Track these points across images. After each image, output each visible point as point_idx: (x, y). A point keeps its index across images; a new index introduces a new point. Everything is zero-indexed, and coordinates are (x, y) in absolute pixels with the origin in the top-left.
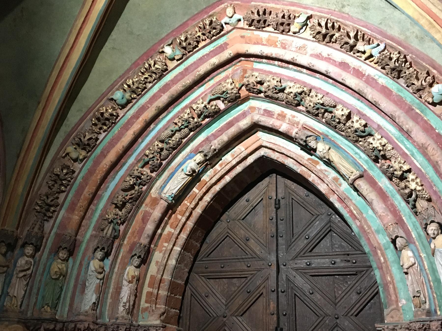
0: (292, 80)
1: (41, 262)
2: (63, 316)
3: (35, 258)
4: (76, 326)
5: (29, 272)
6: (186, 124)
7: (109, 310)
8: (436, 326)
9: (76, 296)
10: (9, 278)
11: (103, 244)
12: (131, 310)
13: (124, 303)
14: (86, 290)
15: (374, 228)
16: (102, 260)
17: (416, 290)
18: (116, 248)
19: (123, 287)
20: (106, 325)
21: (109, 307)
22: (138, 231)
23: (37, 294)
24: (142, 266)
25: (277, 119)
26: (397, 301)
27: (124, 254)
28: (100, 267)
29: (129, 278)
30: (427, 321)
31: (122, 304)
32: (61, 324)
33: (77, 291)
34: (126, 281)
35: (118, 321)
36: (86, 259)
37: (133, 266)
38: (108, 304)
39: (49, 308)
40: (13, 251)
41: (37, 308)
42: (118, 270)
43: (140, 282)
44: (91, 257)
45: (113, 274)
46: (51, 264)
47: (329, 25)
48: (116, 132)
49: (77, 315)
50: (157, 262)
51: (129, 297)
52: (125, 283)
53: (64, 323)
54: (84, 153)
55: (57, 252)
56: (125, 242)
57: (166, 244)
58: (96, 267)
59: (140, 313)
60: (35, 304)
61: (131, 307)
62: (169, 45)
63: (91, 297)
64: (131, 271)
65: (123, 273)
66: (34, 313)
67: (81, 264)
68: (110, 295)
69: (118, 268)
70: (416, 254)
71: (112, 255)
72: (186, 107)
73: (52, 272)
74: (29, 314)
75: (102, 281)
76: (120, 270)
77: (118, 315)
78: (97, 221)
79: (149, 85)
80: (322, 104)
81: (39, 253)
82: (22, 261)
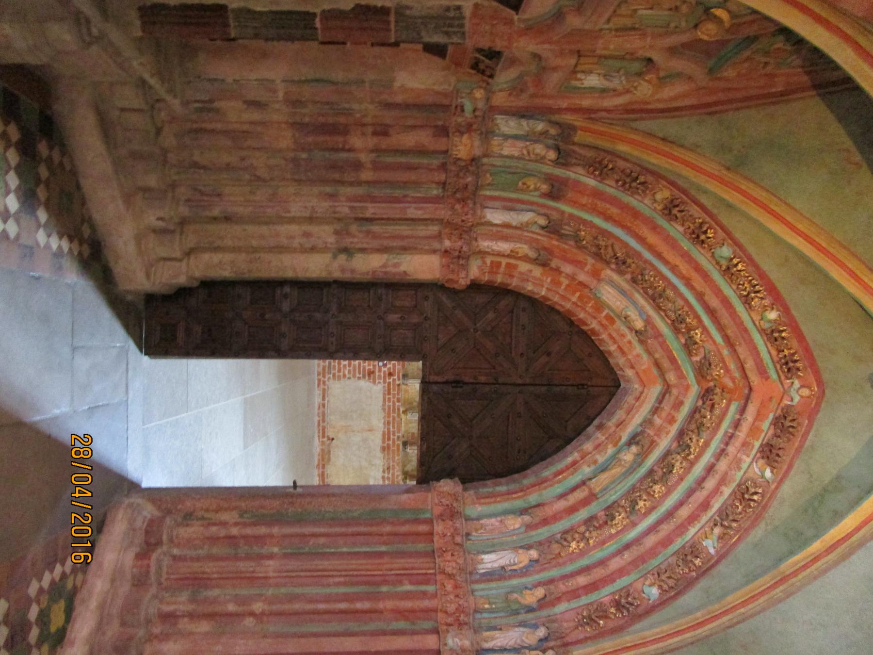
0: (707, 444)
6: (680, 319)
15: (544, 492)
25: (670, 414)
26: (480, 504)
47: (752, 504)
48: (682, 244)
50: (531, 271)
54: (659, 208)
57: (549, 280)
62: (779, 316)
70: (516, 532)
72: (700, 321)
79: (734, 287)
80: (671, 471)
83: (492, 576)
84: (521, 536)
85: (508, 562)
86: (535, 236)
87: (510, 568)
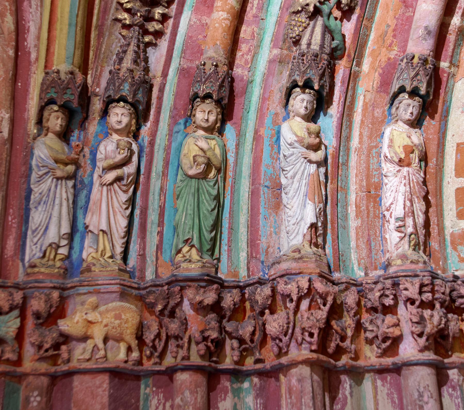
1: (156, 147)
2: (236, 274)
3: (140, 140)
4: (274, 290)
5: (130, 169)
7: (357, 246)
9: (261, 217)
10: (85, 192)
11: (304, 72)
12: (422, 238)
13: (397, 219)
14: (283, 195)
16: (312, 117)
18: (343, 82)
19: (386, 181)
20: (361, 285)
21: (357, 239)
22: (394, 30)
23: (161, 223)
24: (425, 123)
27: (369, 96)
28: (309, 133)
29: (396, 153)
31: (393, 224)
32: (235, 291)
33: (262, 203)
34: (392, 162)
35: (391, 270)
36: (268, 121)
37: (400, 123)
38: (353, 234)
39: (194, 251)
40: (82, 126)
41: (166, 256)
42: (361, 142)
43: (430, 164)
44: (281, 117)
45: (348, 155)
46: (181, 144)
49: (274, 264)
51: (408, 203)
52: (388, 168)
53: (242, 288)
55: (190, 117)
56: (365, 67)
58: (299, 134)
59: (449, 249)
60: (159, 247)
61: (422, 232)
63: (300, 211)
64: (398, 135)
65: (378, 146)
66: (160, 270)
67: (257, 138)
68: (352, 210)
69: (361, 135)
71: (335, 104)
73: (186, 162)
74: (149, 275)
75: (322, 170)
76: (365, 139)
77: (388, 255)
78: (278, 23)
81: (149, 124)
82: (109, 149)
86: (357, 118)
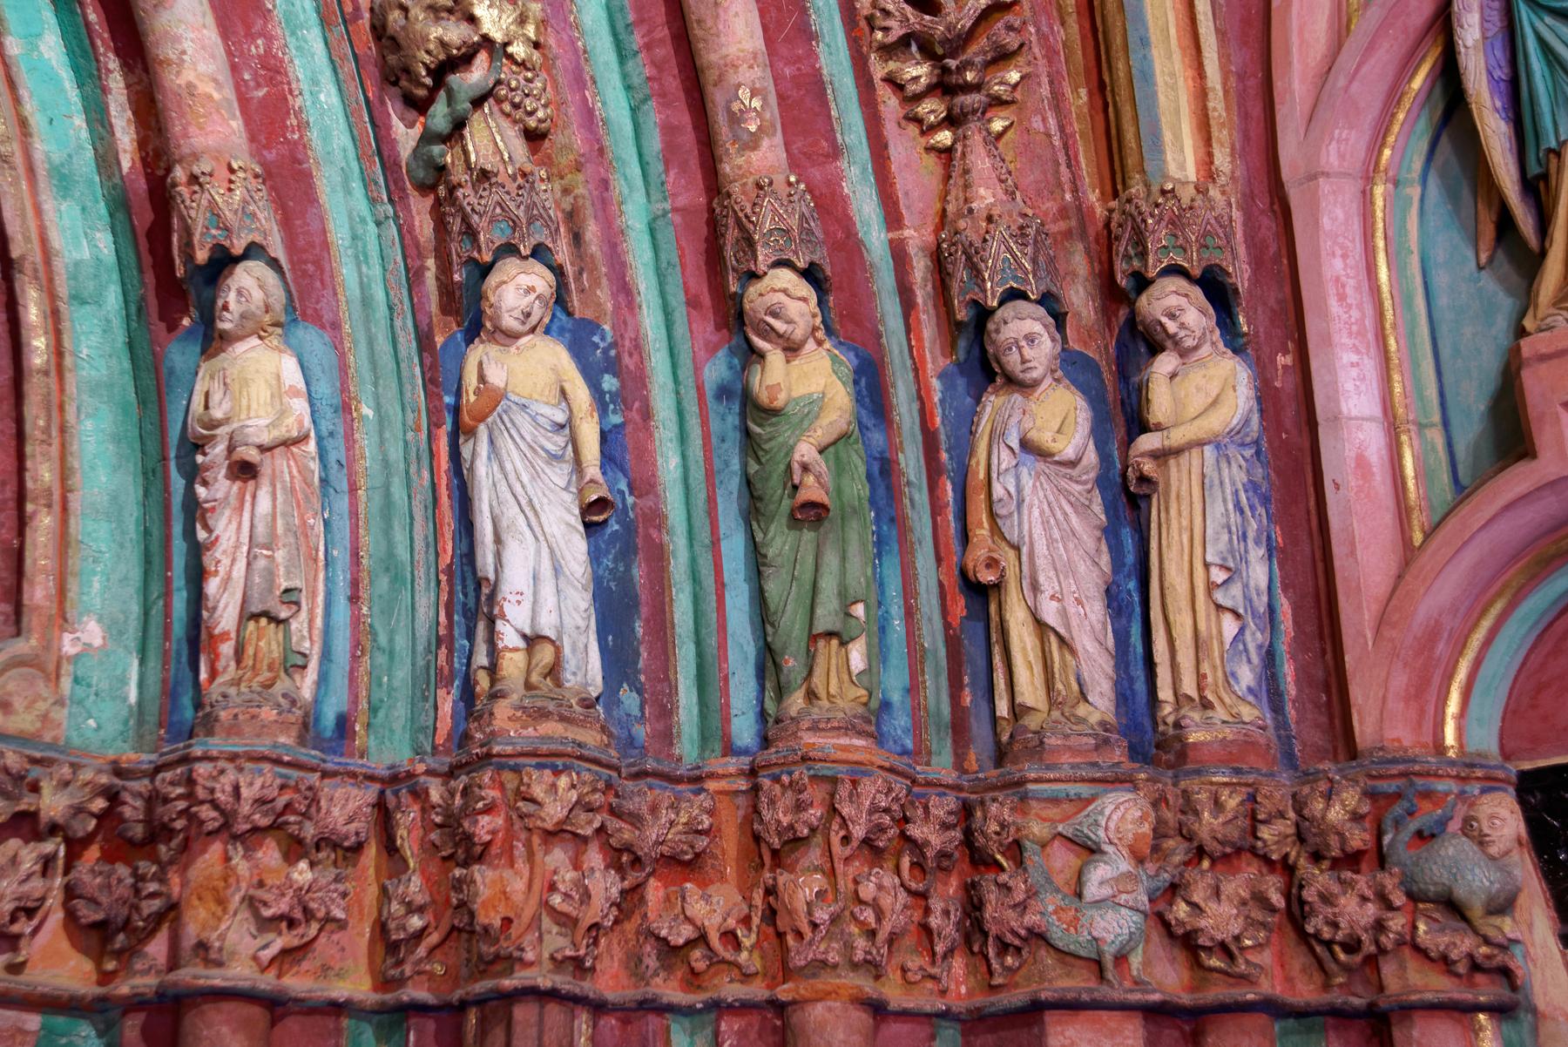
8: (352, 806)
17: (284, 585)
26: (62, 618)
30: (313, 770)
70: (324, 389)
83: (625, 608)
84: (358, 360)
85: (559, 475)
87: (593, 471)
